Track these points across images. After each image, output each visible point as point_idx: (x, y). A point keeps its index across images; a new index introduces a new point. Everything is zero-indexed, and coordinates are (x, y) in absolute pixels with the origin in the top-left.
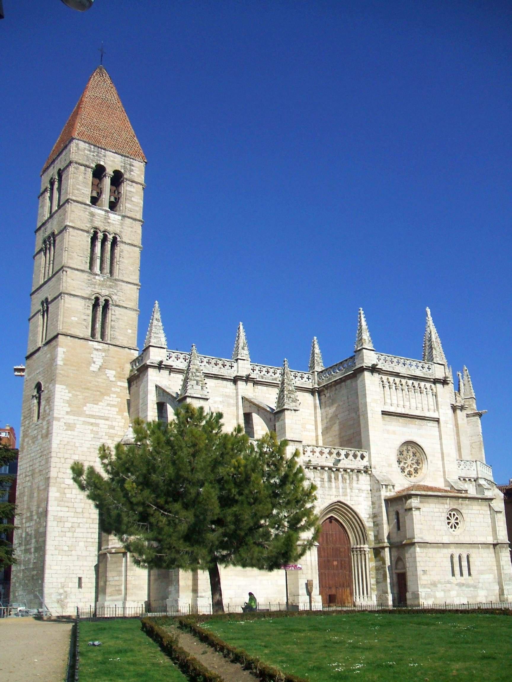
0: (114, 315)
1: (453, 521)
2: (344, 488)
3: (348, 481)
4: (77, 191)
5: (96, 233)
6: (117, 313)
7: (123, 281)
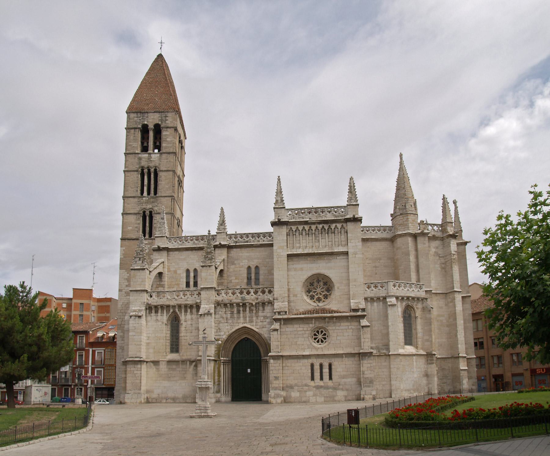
0: (156, 220)
1: (320, 336)
2: (251, 317)
3: (254, 312)
4: (129, 147)
5: (143, 170)
6: (158, 218)
7: (161, 197)
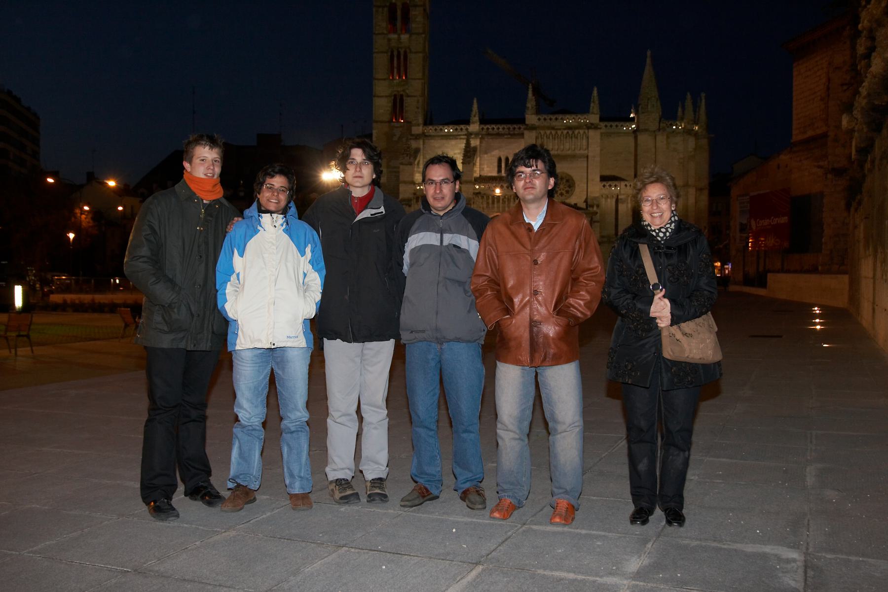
3: (507, 203)
